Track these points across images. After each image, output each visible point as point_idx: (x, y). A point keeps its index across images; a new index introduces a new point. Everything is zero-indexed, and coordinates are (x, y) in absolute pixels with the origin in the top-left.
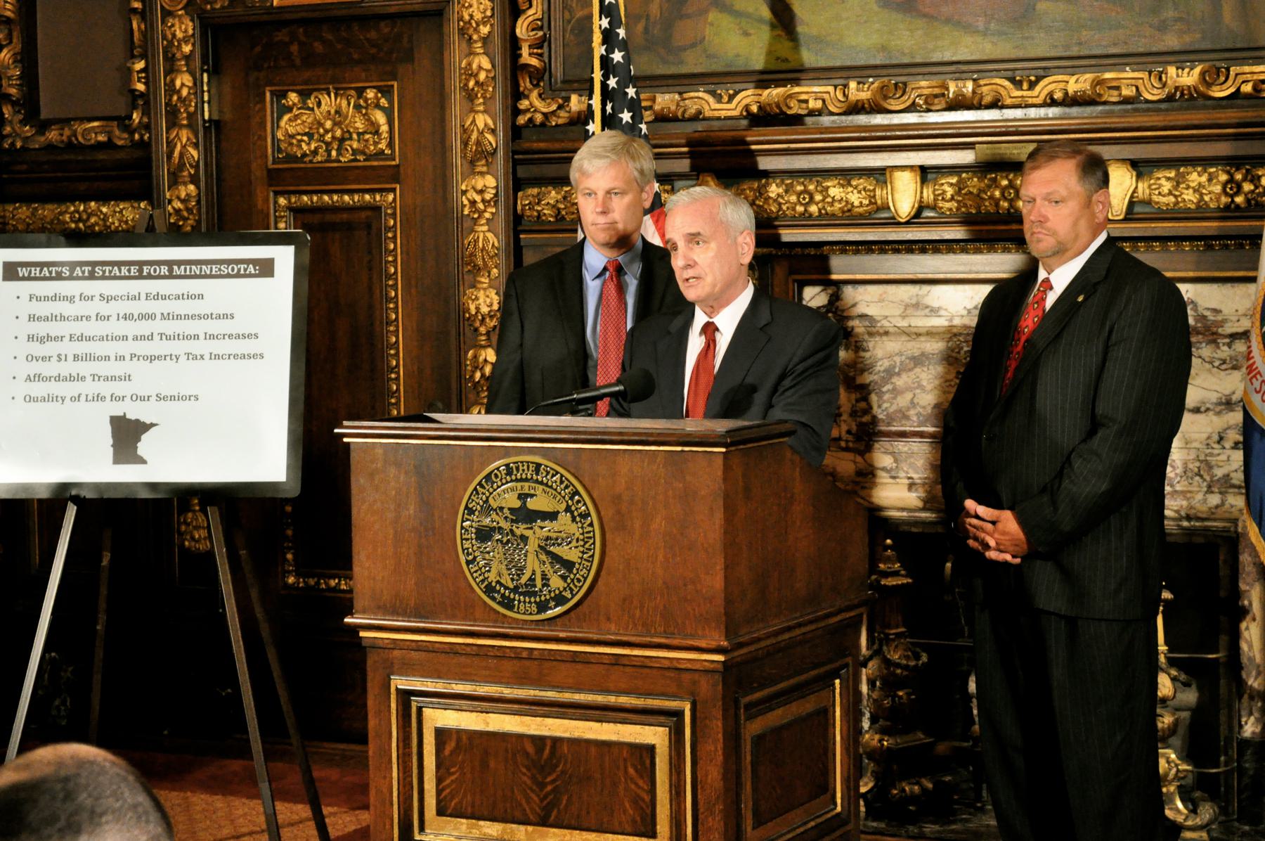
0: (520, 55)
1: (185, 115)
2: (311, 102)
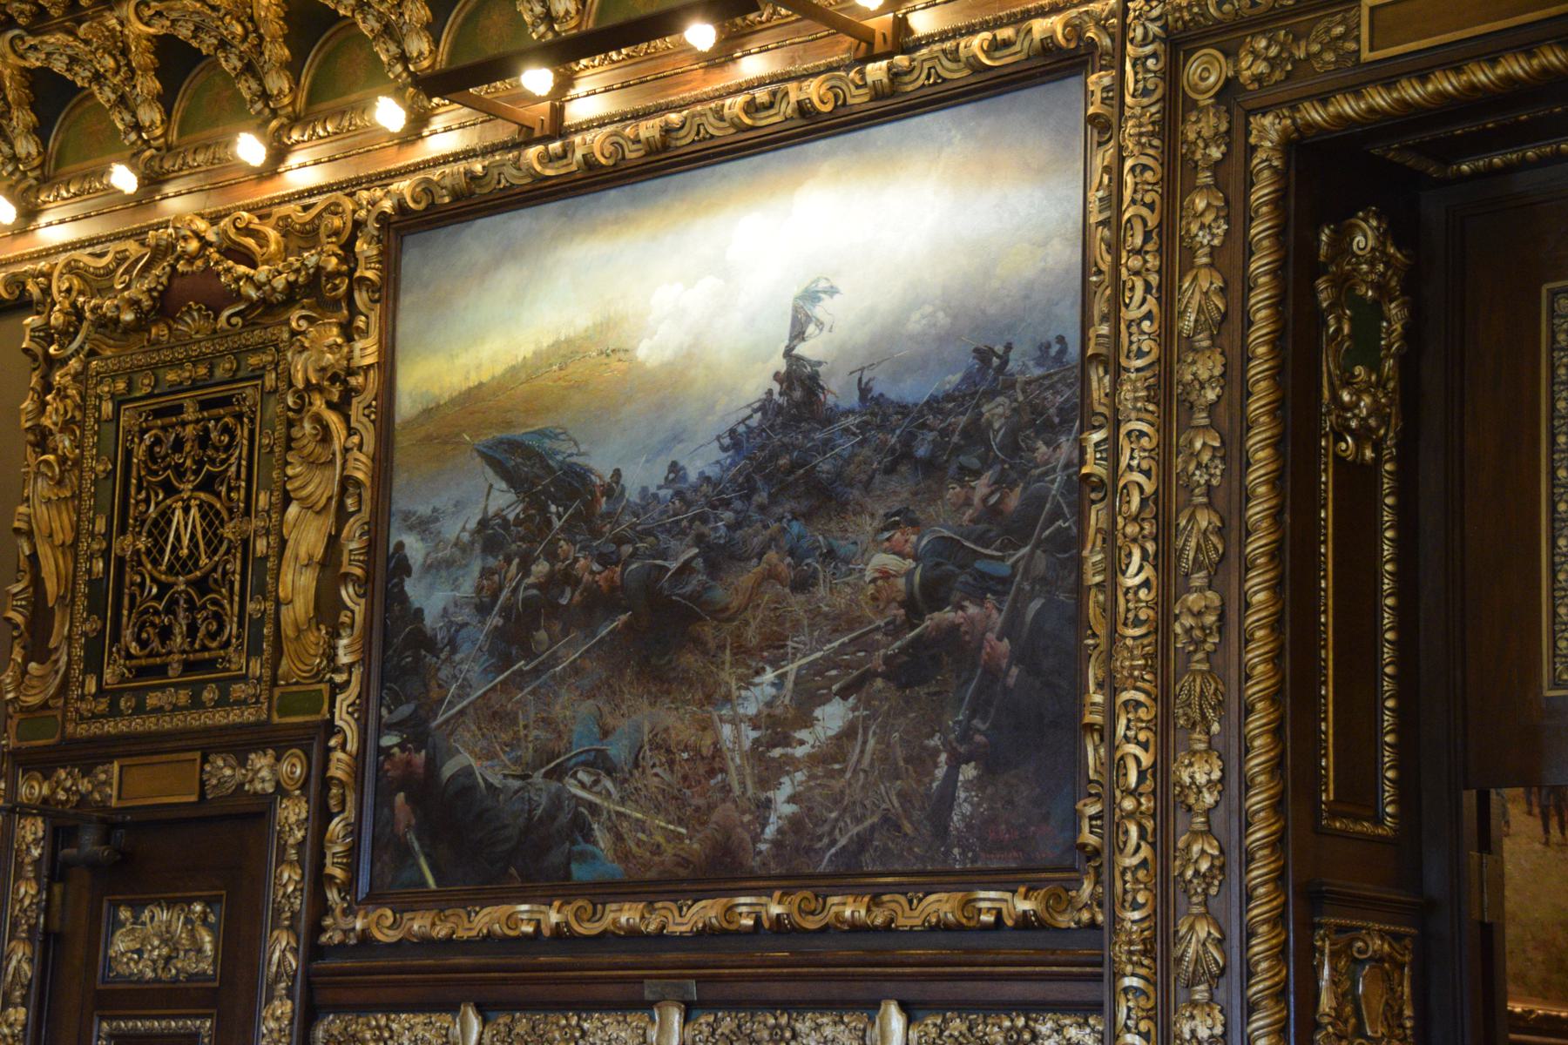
0: (324, 865)
1: (25, 927)
2: (146, 915)
